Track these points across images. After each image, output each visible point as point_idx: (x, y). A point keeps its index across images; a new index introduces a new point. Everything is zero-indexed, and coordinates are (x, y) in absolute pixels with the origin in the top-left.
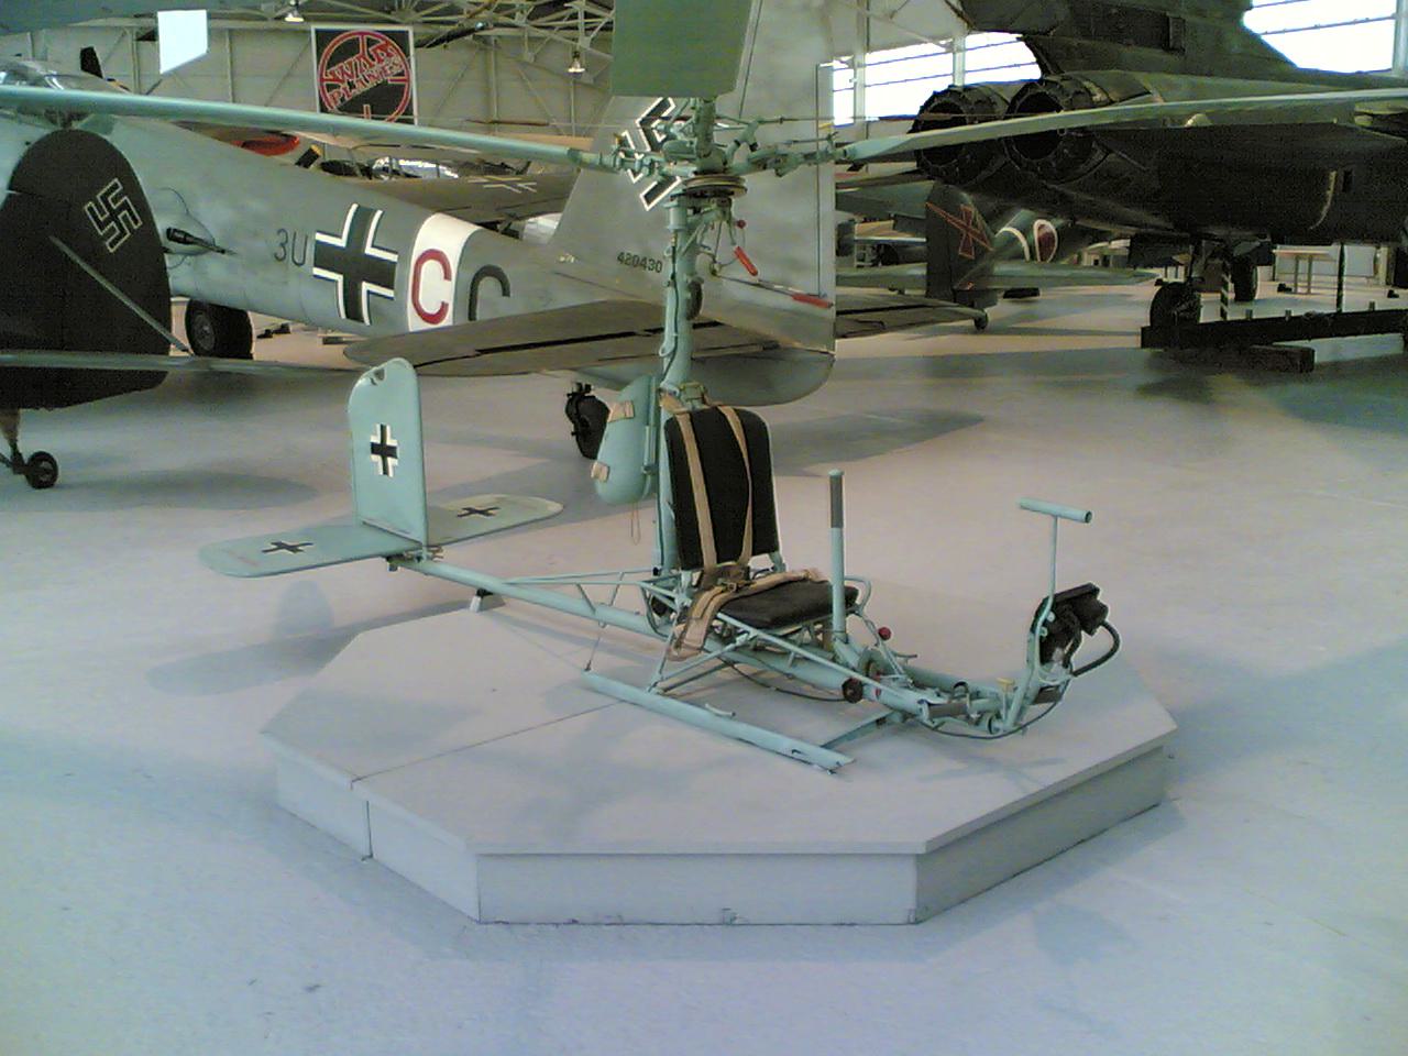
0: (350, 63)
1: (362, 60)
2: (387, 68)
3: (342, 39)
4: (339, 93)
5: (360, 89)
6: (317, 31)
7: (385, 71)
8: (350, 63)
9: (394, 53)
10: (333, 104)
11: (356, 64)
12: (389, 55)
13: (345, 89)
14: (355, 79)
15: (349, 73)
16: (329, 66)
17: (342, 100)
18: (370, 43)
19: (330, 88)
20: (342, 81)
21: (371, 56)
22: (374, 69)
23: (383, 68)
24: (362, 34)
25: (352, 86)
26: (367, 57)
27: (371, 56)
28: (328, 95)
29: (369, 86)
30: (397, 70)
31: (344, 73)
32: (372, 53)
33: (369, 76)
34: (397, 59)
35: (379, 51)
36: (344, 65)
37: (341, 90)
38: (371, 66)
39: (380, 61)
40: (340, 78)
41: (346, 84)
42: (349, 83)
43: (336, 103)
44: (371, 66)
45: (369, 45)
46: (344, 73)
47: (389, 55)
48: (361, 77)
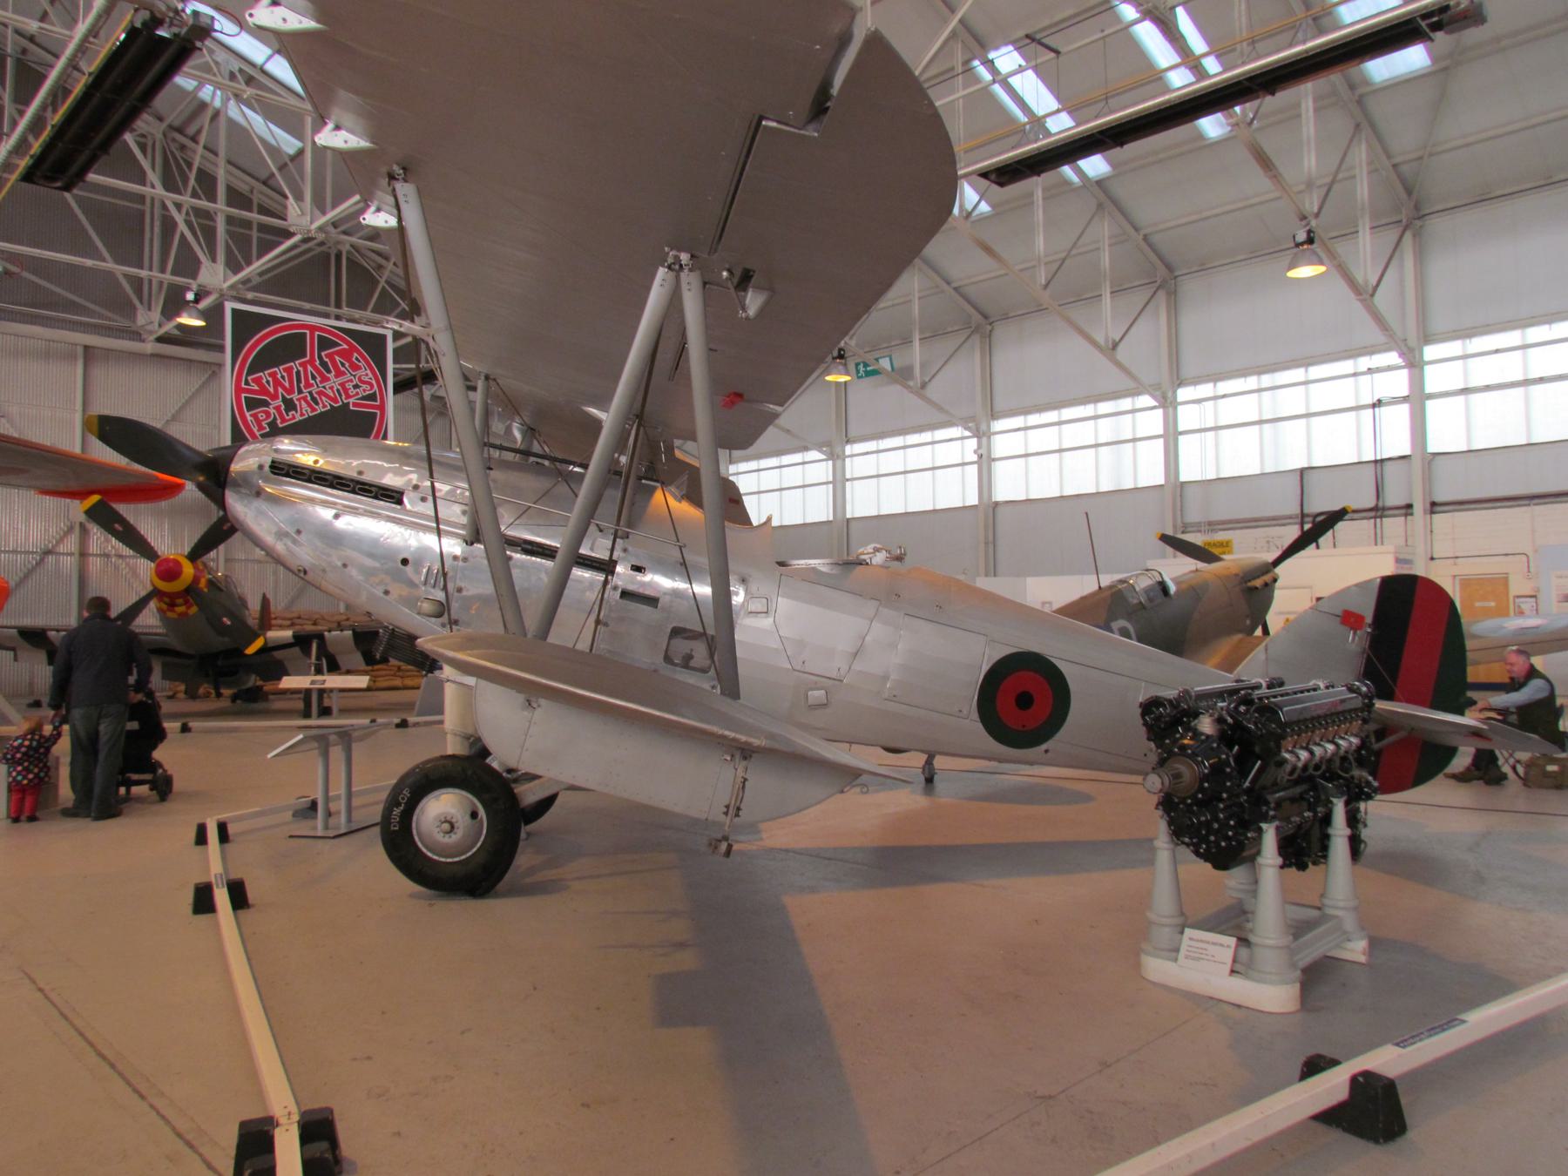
2: (349, 386)
4: (268, 414)
6: (234, 311)
9: (362, 364)
11: (298, 373)
13: (278, 408)
16: (257, 366)
18: (325, 344)
19: (252, 404)
20: (275, 397)
22: (327, 385)
23: (342, 385)
24: (313, 328)
25: (290, 406)
28: (248, 415)
29: (320, 409)
30: (365, 390)
31: (277, 383)
33: (320, 393)
34: (366, 373)
36: (280, 371)
39: (339, 374)
41: (279, 402)
43: (261, 428)
45: (321, 349)
46: (277, 383)
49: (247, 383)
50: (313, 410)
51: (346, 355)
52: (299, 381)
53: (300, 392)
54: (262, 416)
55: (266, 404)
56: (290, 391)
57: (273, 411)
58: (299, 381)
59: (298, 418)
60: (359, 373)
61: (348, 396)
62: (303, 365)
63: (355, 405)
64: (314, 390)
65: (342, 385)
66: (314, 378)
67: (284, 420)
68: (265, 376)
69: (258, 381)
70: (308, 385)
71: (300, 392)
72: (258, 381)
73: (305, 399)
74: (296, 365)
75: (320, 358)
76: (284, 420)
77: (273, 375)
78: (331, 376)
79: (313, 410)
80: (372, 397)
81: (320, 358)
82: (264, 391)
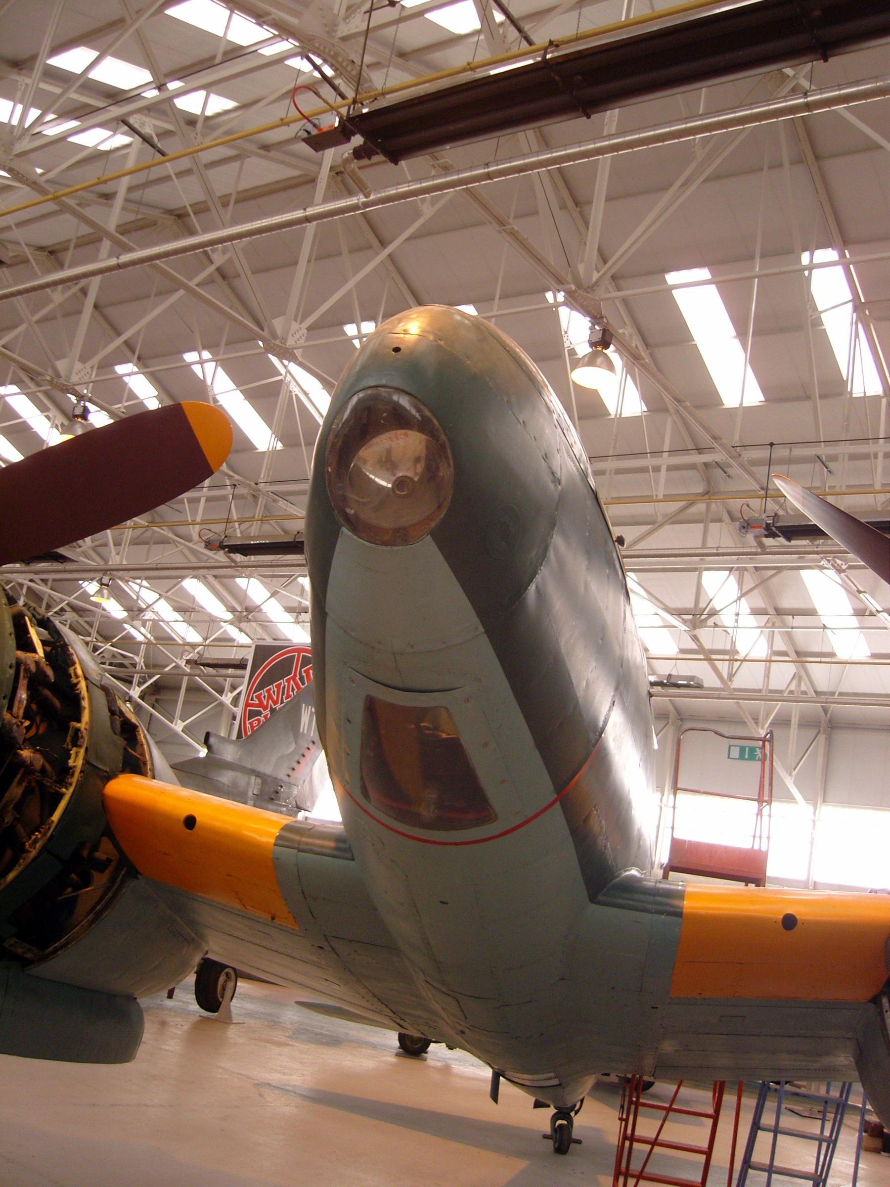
0: (278, 686)
1: (292, 682)
4: (259, 720)
13: (265, 717)
15: (275, 698)
19: (253, 714)
20: (265, 708)
21: (302, 679)
26: (297, 678)
32: (304, 674)
36: (273, 687)
37: (262, 719)
52: (283, 694)
54: (255, 723)
55: (259, 713)
56: (275, 703)
58: (283, 694)
62: (288, 681)
68: (264, 692)
69: (259, 697)
72: (259, 697)
74: (283, 682)
82: (261, 704)
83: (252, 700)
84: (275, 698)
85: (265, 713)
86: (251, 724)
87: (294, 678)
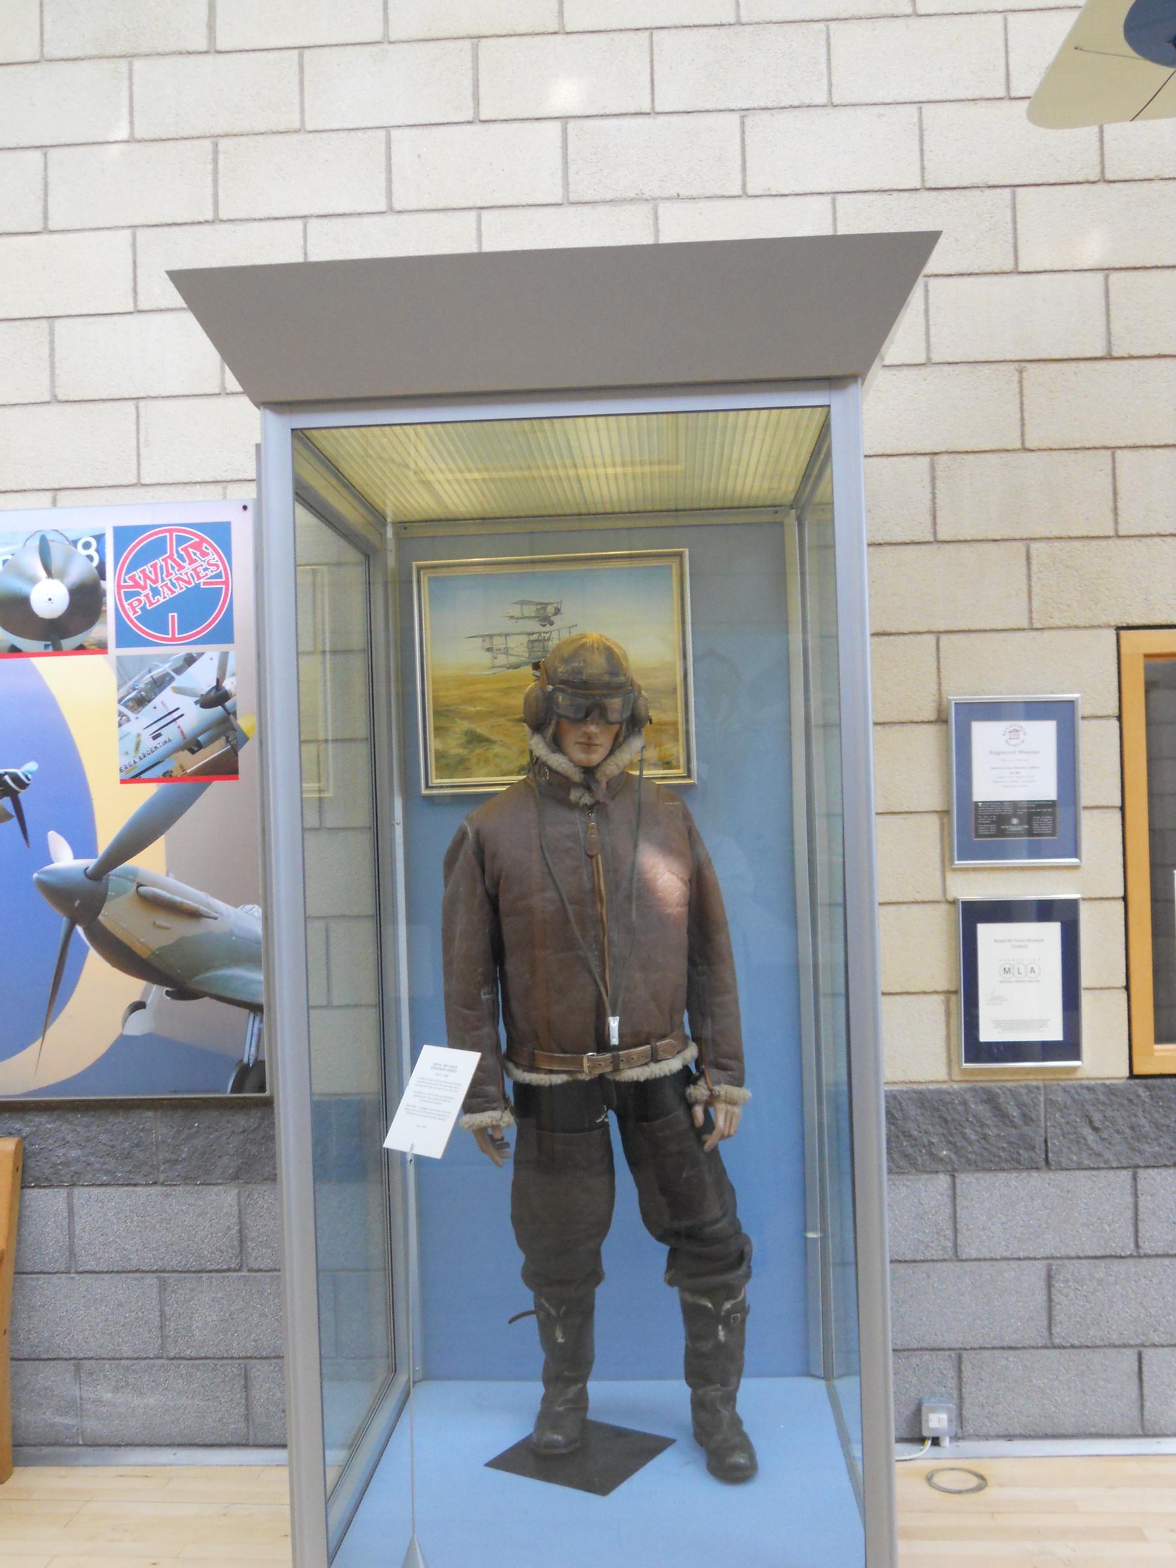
0: (154, 566)
1: (169, 561)
3: (148, 537)
4: (140, 601)
5: (168, 595)
7: (197, 574)
8: (154, 566)
9: (210, 551)
10: (131, 614)
12: (204, 554)
13: (147, 596)
14: (159, 585)
15: (153, 577)
17: (143, 609)
18: (181, 541)
19: (129, 596)
20: (144, 588)
21: (180, 557)
22: (183, 572)
23: (194, 570)
25: (156, 592)
26: (175, 557)
27: (180, 557)
29: (178, 591)
31: (146, 577)
33: (178, 579)
34: (213, 558)
35: (190, 550)
36: (148, 568)
37: (142, 598)
38: (181, 568)
39: (192, 561)
40: (142, 583)
41: (148, 591)
42: (152, 589)
43: (135, 612)
44: (181, 568)
45: (178, 546)
46: (146, 577)
47: (204, 554)
48: (167, 581)
49: (125, 581)
50: (173, 592)
51: (197, 546)
53: (163, 580)
55: (139, 594)
56: (155, 582)
57: (142, 598)
59: (162, 600)
60: (207, 558)
61: (199, 578)
62: (165, 560)
63: (205, 583)
64: (173, 577)
65: (194, 570)
66: (173, 568)
67: (151, 604)
68: (137, 574)
69: (132, 578)
70: (169, 574)
71: (163, 580)
72: (132, 578)
73: (166, 585)
74: (159, 561)
75: (177, 552)
76: (151, 604)
77: (143, 572)
78: (186, 564)
79: (173, 592)
80: (219, 576)
81: (177, 552)
82: (137, 585)
83: (125, 581)
84: (153, 577)
85: (144, 593)
86: (131, 605)
87: (171, 557)
